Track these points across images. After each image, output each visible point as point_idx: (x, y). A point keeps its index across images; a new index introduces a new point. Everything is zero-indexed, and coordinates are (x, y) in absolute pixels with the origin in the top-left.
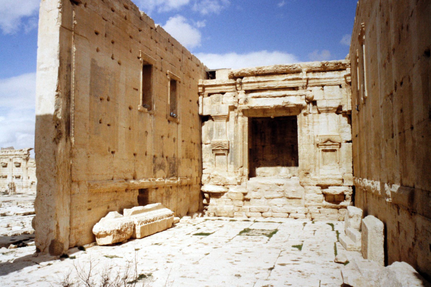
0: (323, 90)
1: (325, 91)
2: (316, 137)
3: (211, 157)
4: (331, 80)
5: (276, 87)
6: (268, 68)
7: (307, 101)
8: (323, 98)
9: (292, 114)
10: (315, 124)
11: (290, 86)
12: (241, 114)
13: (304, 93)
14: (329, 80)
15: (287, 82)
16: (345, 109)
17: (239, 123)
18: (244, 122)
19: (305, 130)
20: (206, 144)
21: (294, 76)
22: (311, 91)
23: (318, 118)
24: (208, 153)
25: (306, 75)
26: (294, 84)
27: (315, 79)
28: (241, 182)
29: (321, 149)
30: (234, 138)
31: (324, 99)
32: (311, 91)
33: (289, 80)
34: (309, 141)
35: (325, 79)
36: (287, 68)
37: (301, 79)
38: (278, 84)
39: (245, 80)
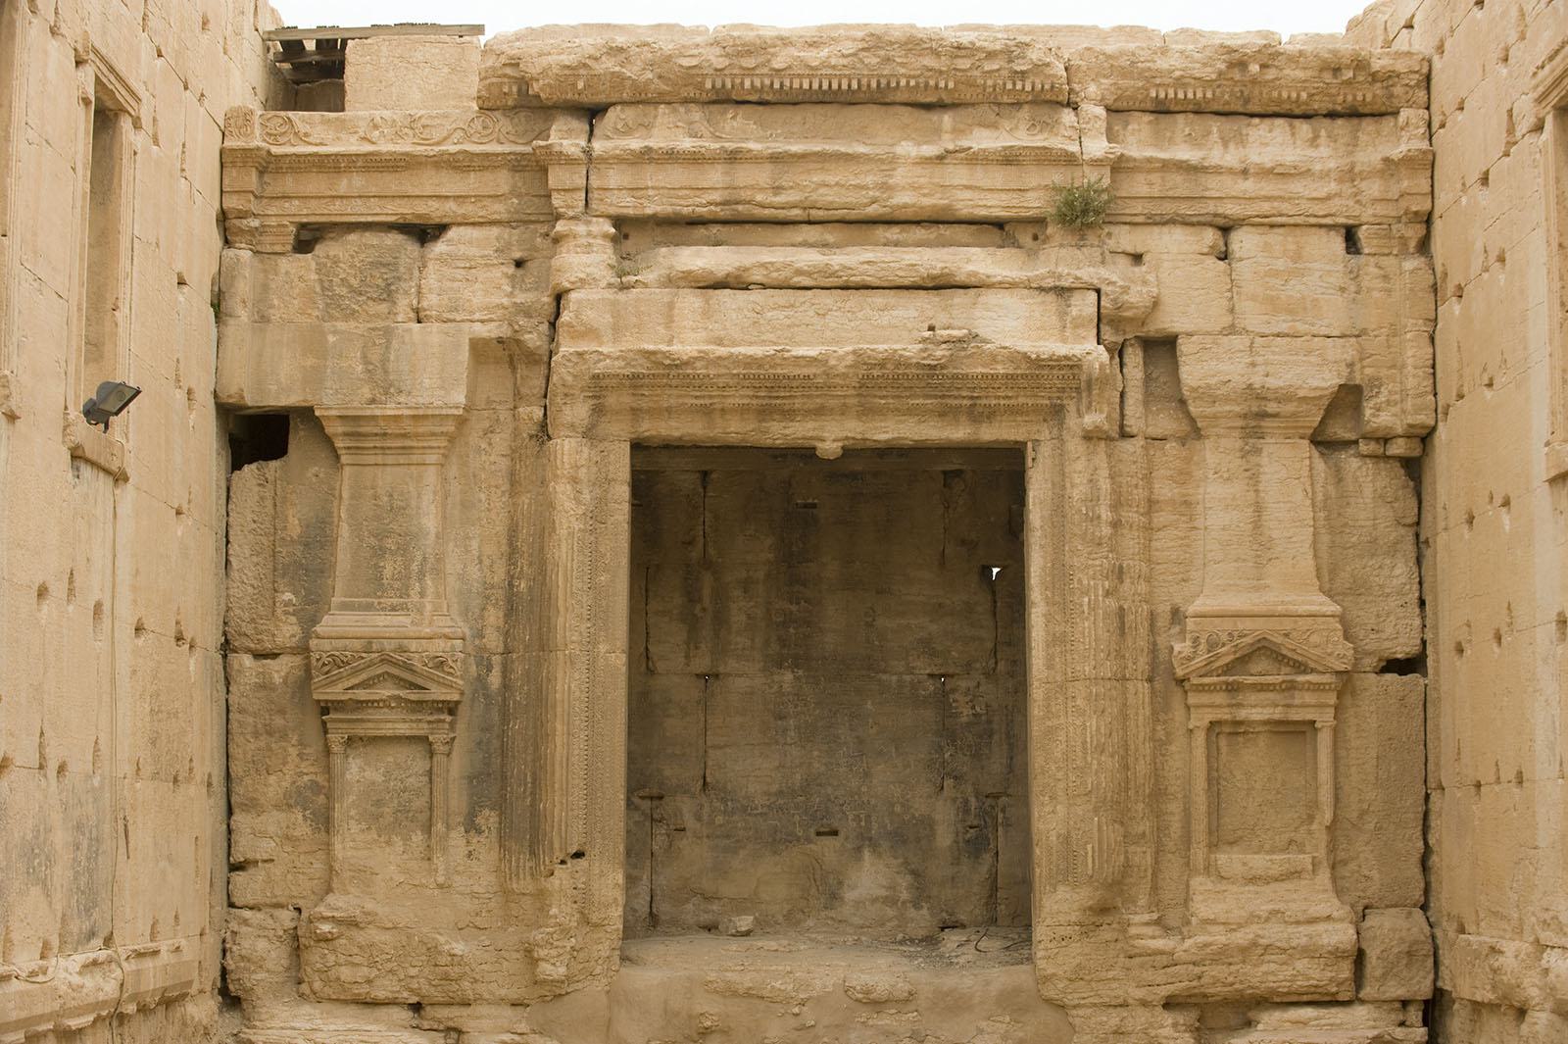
0: (1224, 257)
1: (1243, 269)
2: (1162, 622)
3: (305, 767)
4: (1297, 187)
5: (873, 210)
6: (814, 57)
7: (1108, 335)
8: (1227, 320)
9: (991, 433)
10: (1161, 518)
11: (983, 212)
12: (577, 412)
13: (1089, 273)
14: (1269, 188)
15: (958, 175)
16: (1381, 415)
17: (562, 492)
18: (605, 482)
19: (1088, 569)
20: (258, 655)
21: (1015, 135)
22: (1137, 258)
23: (1184, 476)
24: (284, 737)
25: (1111, 137)
26: (1013, 199)
27: (1167, 166)
28: (569, 979)
29: (1200, 719)
30: (511, 611)
31: (1231, 330)
32: (1137, 258)
33: (975, 159)
34: (1120, 655)
35: (1244, 172)
36: (964, 64)
37: (1070, 160)
38: (885, 187)
39: (614, 138)
